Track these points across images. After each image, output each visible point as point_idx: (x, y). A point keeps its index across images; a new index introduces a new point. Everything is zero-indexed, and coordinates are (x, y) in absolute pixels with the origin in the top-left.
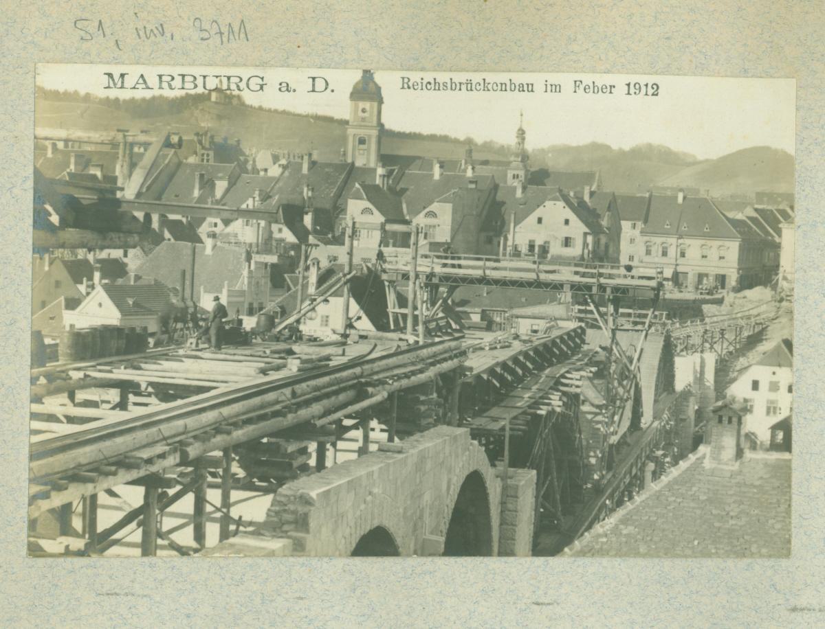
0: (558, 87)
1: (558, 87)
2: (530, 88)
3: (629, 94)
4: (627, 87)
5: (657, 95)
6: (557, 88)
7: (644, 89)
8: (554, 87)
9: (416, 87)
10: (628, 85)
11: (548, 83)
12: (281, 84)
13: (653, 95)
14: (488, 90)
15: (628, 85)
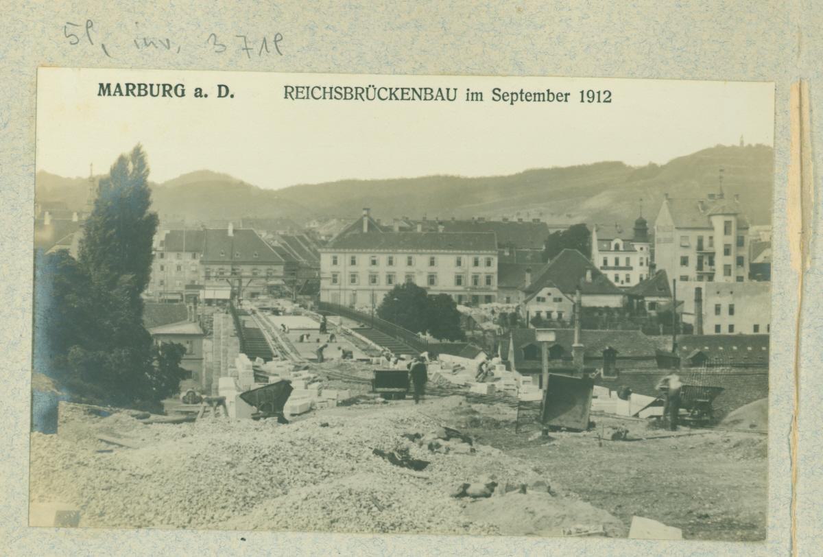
0: (479, 95)
1: (479, 95)
2: (445, 95)
3: (582, 101)
4: (581, 94)
5: (610, 101)
6: (476, 96)
7: (596, 95)
8: (475, 96)
9: (529, 98)
10: (582, 92)
11: (470, 92)
12: (196, 90)
13: (605, 101)
14: (397, 99)
15: (582, 92)
